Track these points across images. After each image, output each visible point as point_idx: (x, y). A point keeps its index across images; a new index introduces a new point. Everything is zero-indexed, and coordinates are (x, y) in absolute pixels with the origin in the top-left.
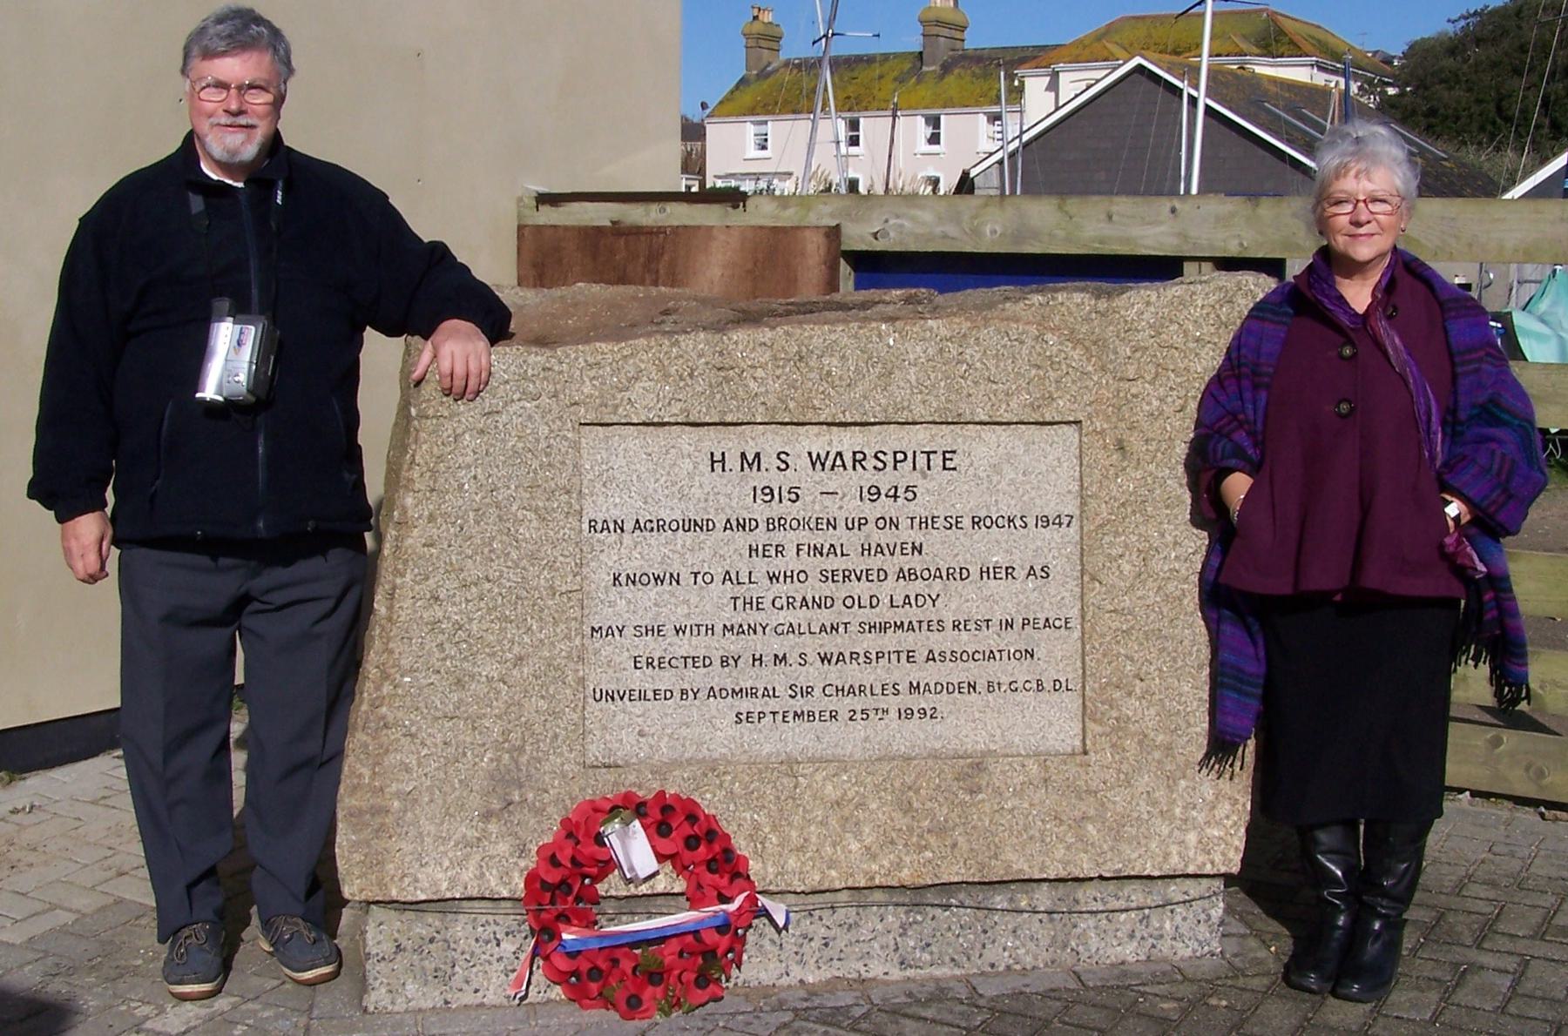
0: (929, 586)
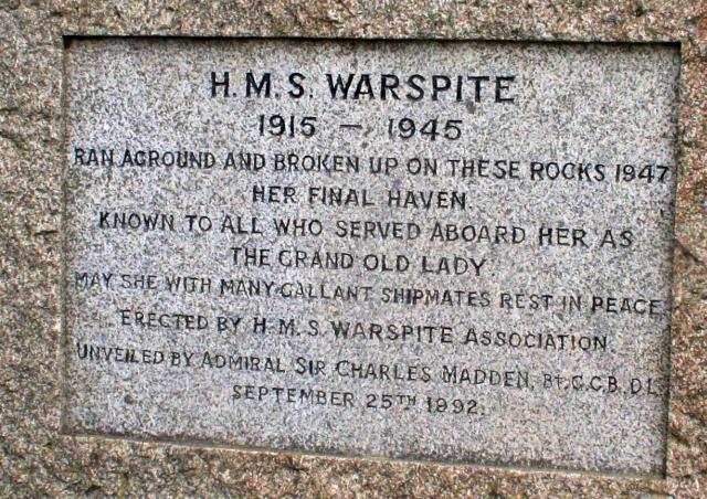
0: (472, 249)
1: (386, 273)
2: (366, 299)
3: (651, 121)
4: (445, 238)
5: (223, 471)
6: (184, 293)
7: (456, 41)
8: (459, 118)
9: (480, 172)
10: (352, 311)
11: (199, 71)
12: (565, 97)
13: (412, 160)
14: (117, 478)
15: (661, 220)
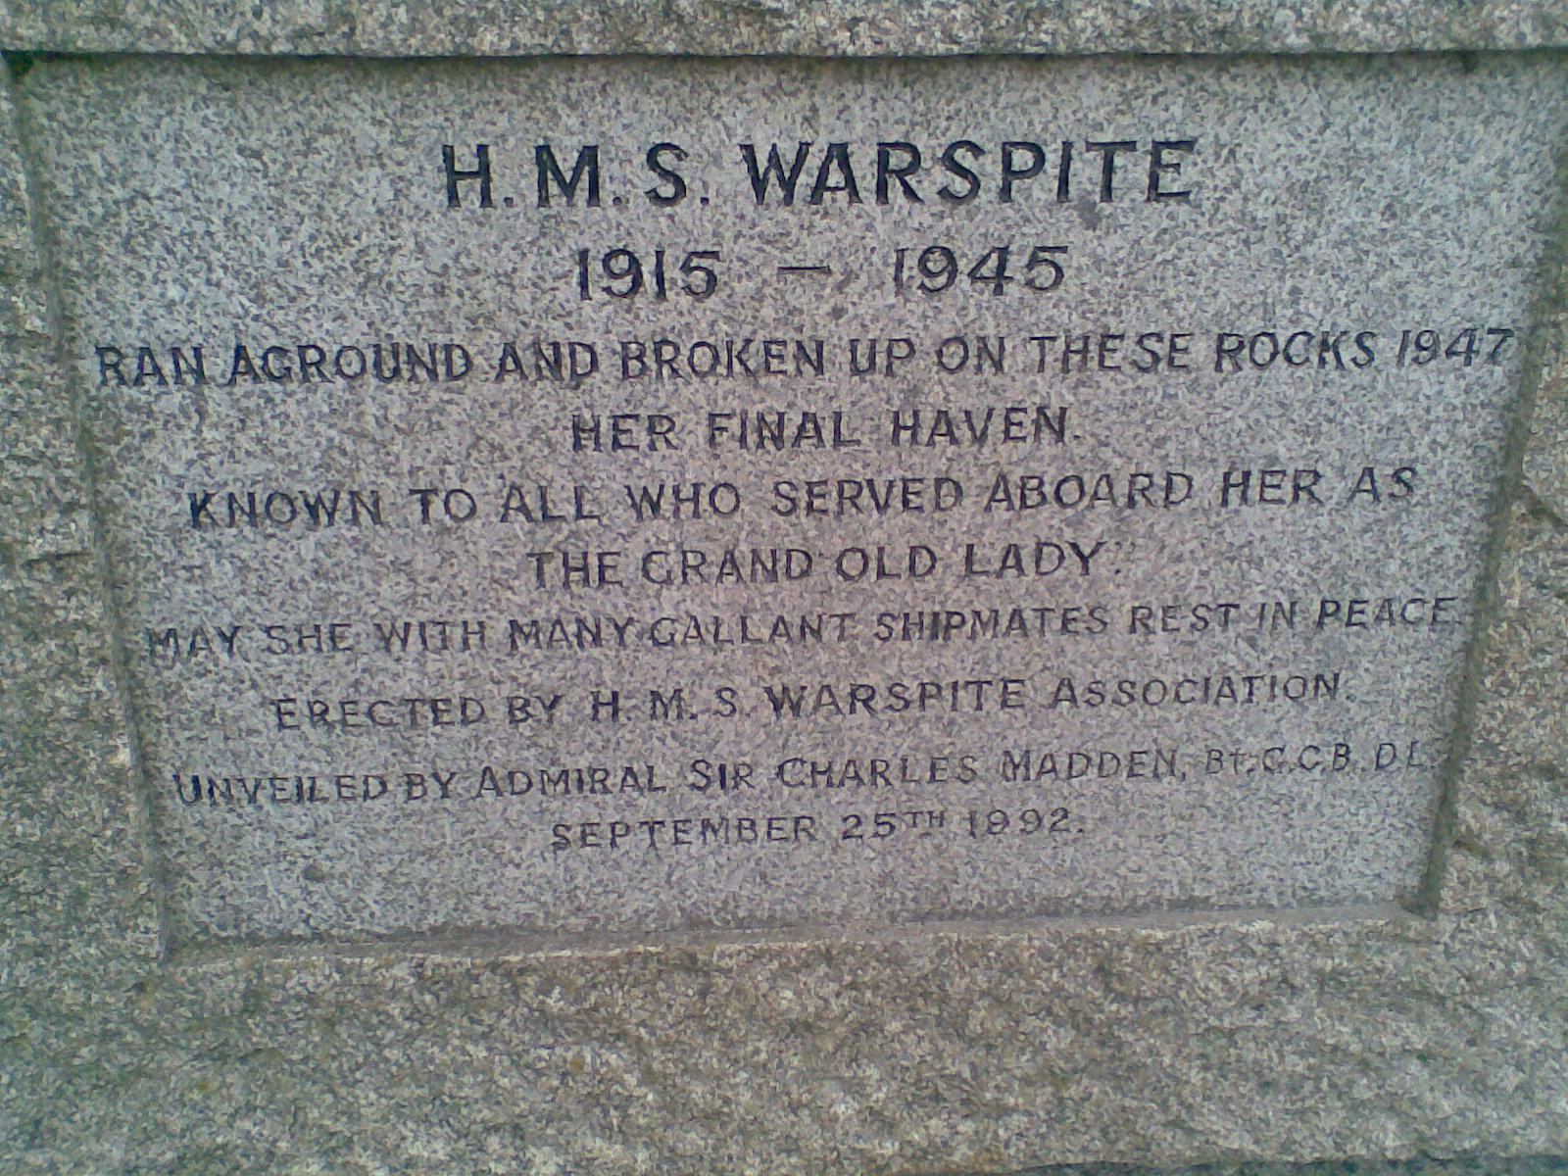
0: (1076, 523)
1: (886, 582)
2: (841, 638)
3: (1492, 232)
4: (1017, 503)
5: (548, 993)
6: (422, 654)
7: (1075, 57)
8: (1062, 241)
9: (1102, 358)
10: (809, 665)
11: (408, 144)
12: (1307, 183)
13: (947, 342)
14: (308, 1028)
15: (1481, 442)
